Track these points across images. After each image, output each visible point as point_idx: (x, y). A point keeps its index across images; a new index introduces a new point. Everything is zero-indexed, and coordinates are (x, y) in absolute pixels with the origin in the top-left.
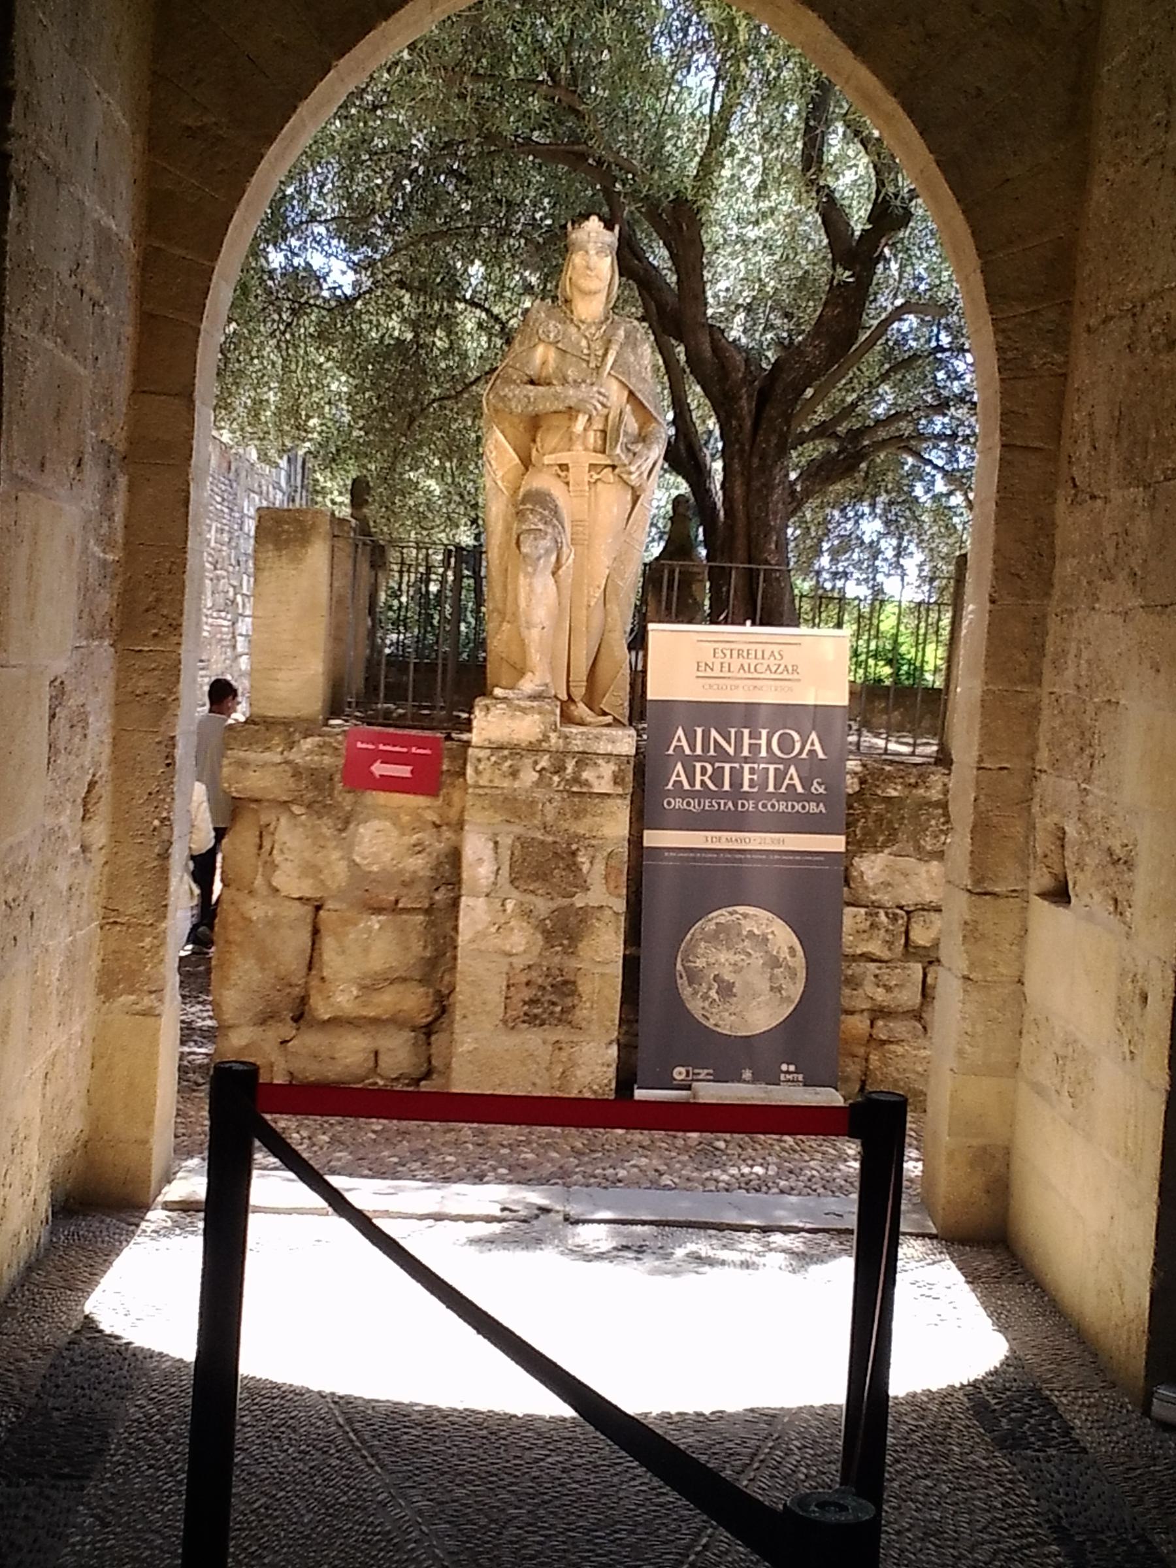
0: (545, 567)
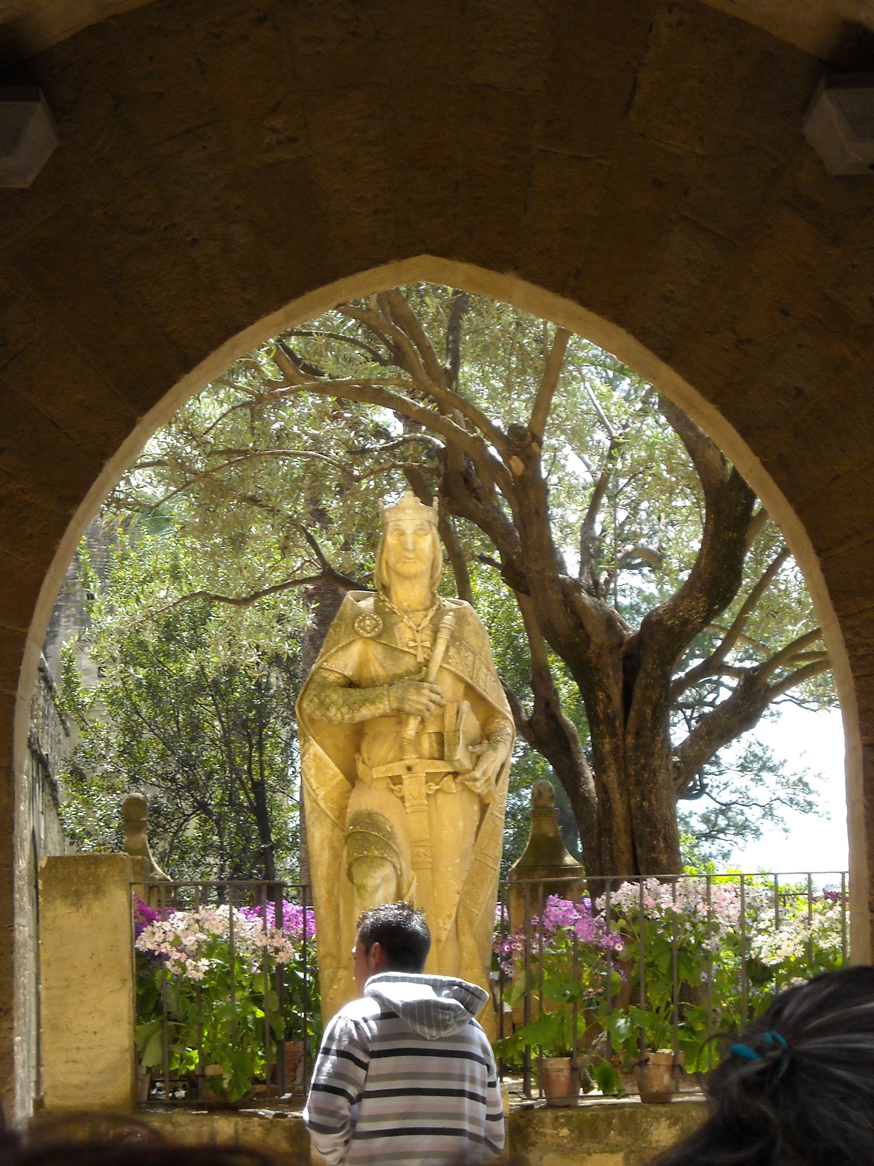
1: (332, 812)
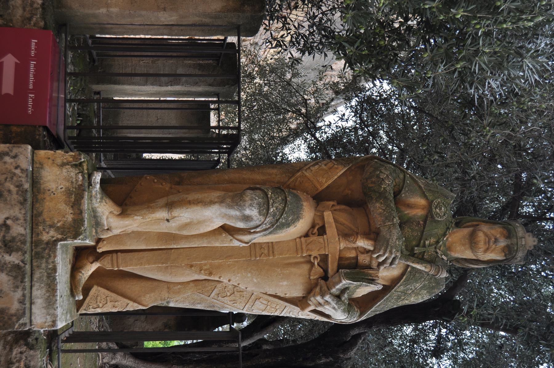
0: (230, 217)
1: (293, 181)
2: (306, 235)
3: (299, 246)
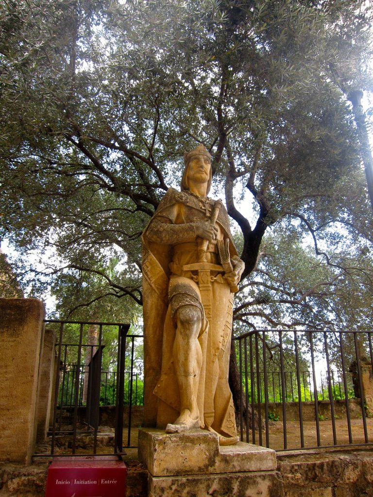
1: (158, 290)
2: (197, 283)
3: (205, 289)
